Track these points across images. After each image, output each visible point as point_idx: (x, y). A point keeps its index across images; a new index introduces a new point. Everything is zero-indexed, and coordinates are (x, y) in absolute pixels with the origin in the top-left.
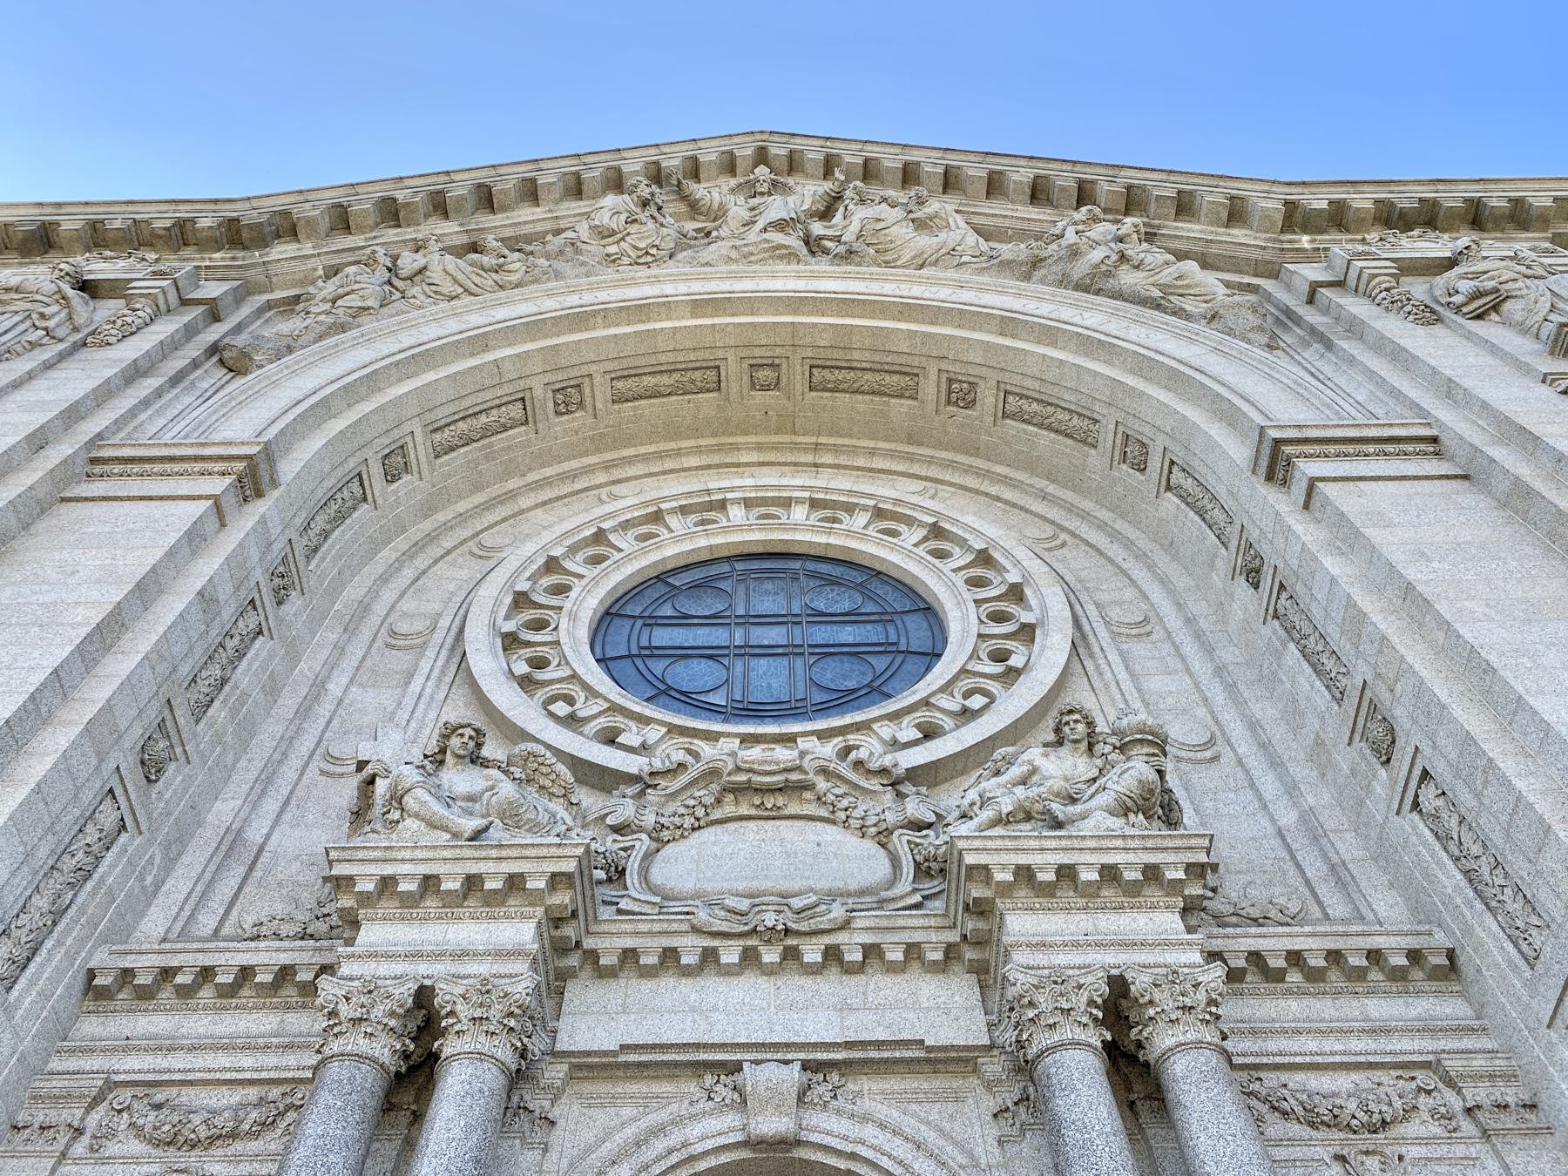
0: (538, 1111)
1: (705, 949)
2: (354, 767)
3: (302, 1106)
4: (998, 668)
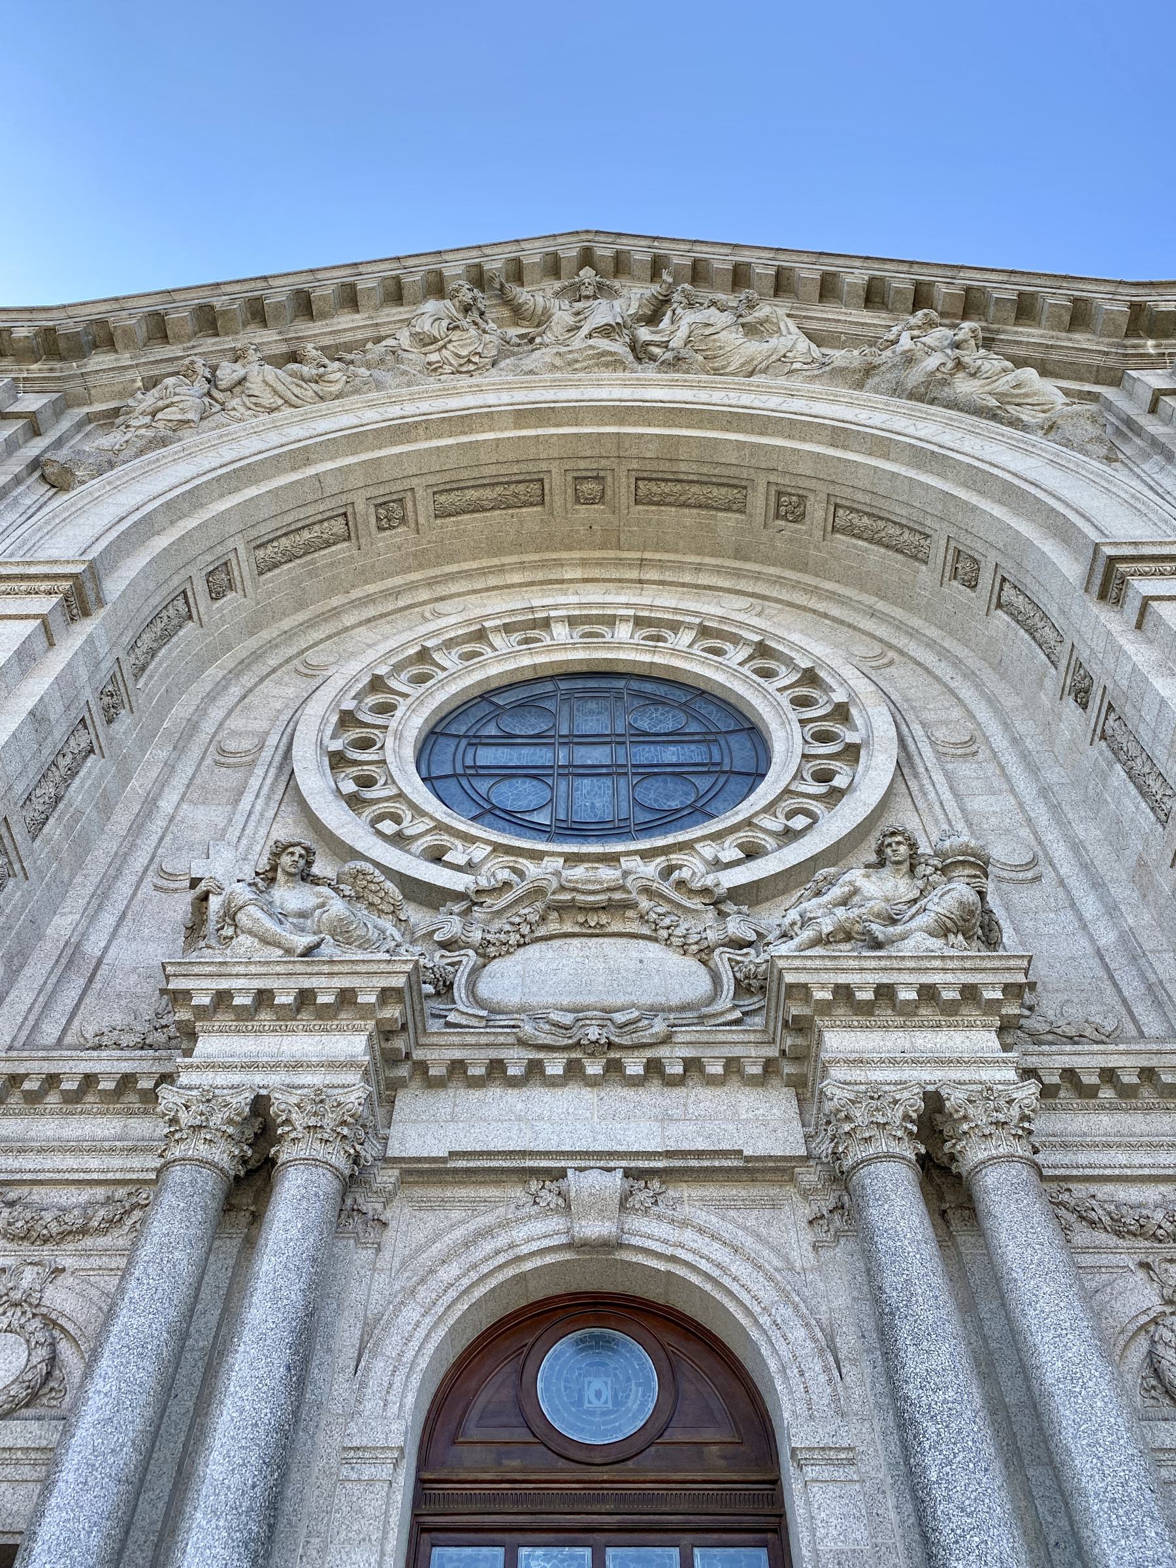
0: (371, 1213)
1: (530, 1061)
2: (187, 883)
3: (146, 1205)
4: (821, 789)
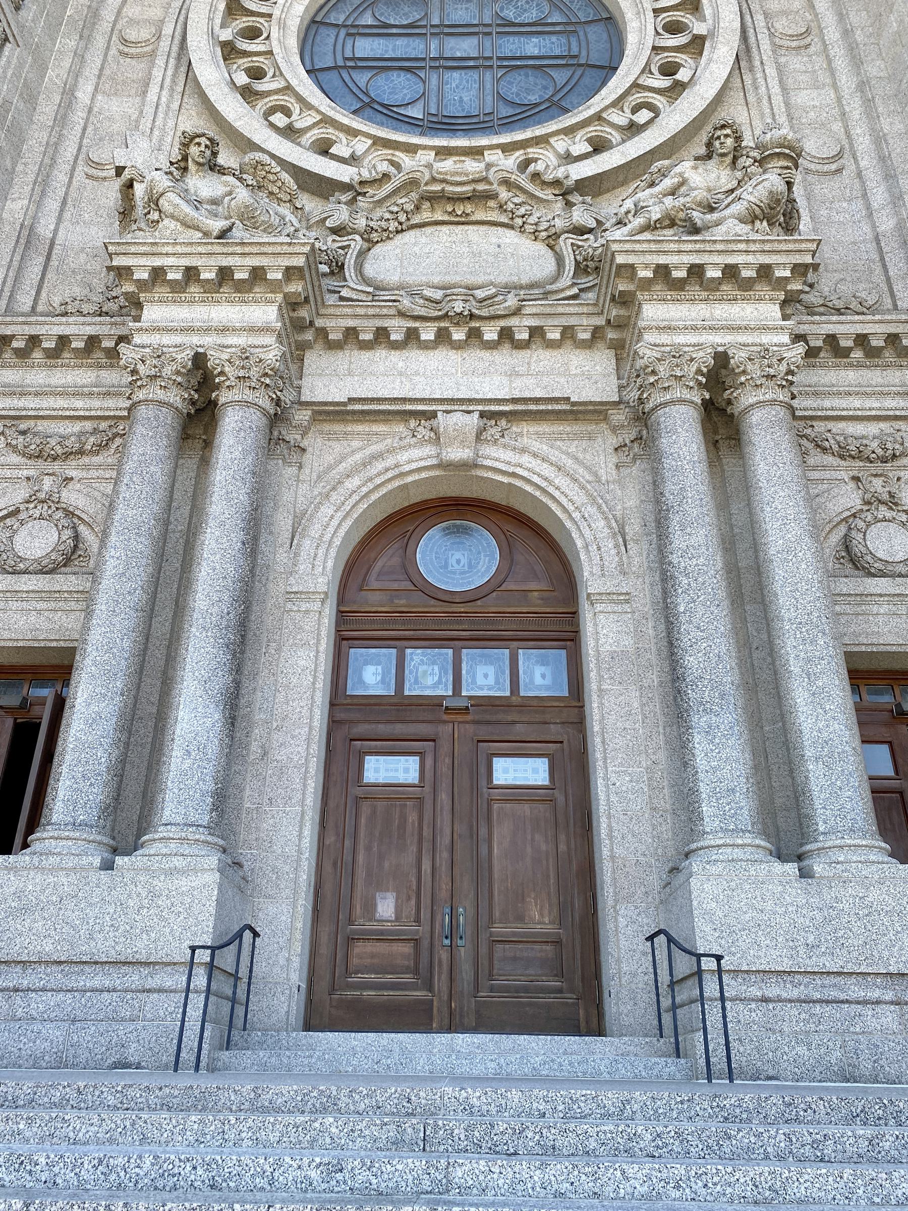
0: (292, 442)
1: (409, 329)
2: (113, 172)
3: (124, 435)
4: (663, 83)
